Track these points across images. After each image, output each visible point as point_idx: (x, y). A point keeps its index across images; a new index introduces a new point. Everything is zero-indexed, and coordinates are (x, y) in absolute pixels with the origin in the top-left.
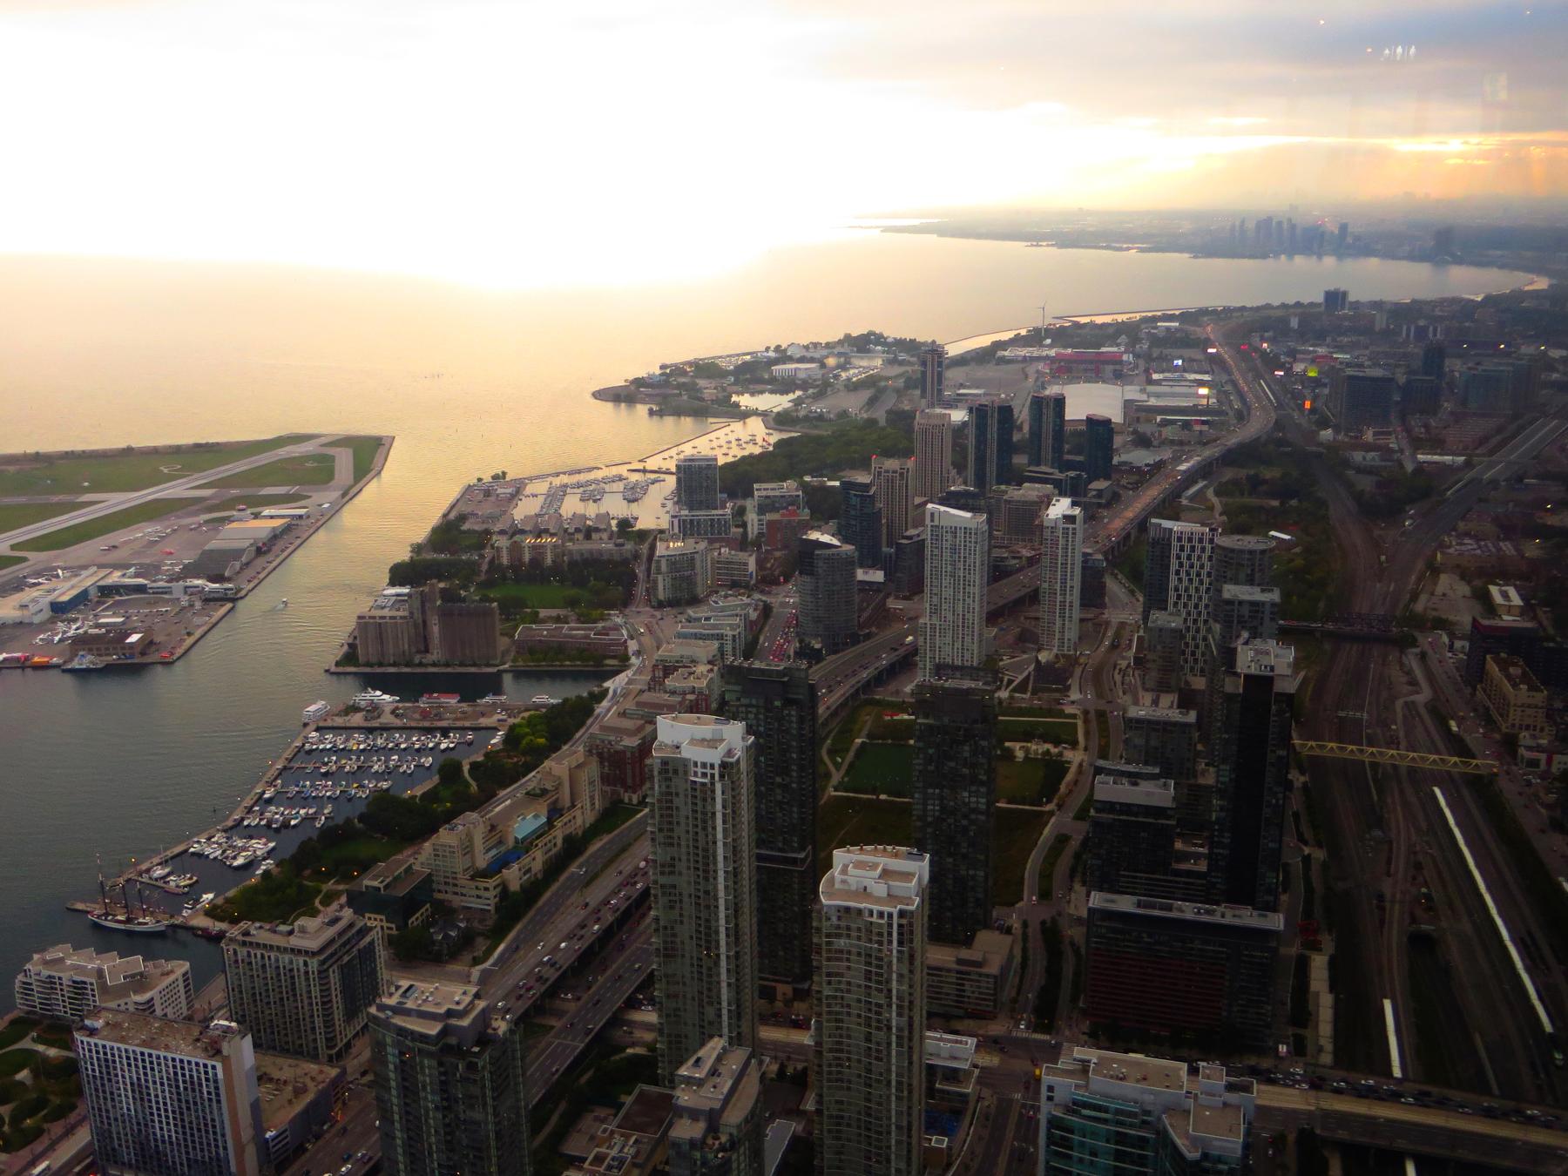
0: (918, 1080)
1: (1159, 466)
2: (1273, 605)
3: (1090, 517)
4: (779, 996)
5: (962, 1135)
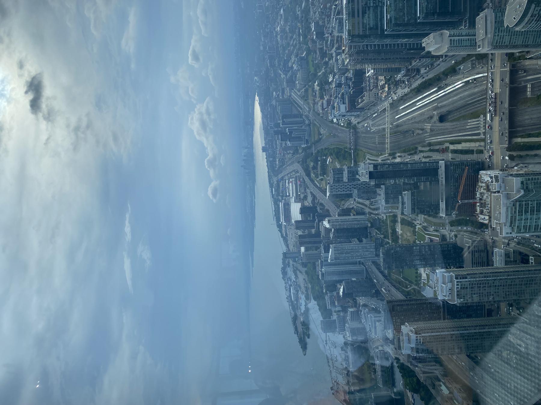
0: (511, 268)
1: (311, 193)
2: (348, 168)
3: (329, 216)
4: (490, 307)
5: (528, 253)
